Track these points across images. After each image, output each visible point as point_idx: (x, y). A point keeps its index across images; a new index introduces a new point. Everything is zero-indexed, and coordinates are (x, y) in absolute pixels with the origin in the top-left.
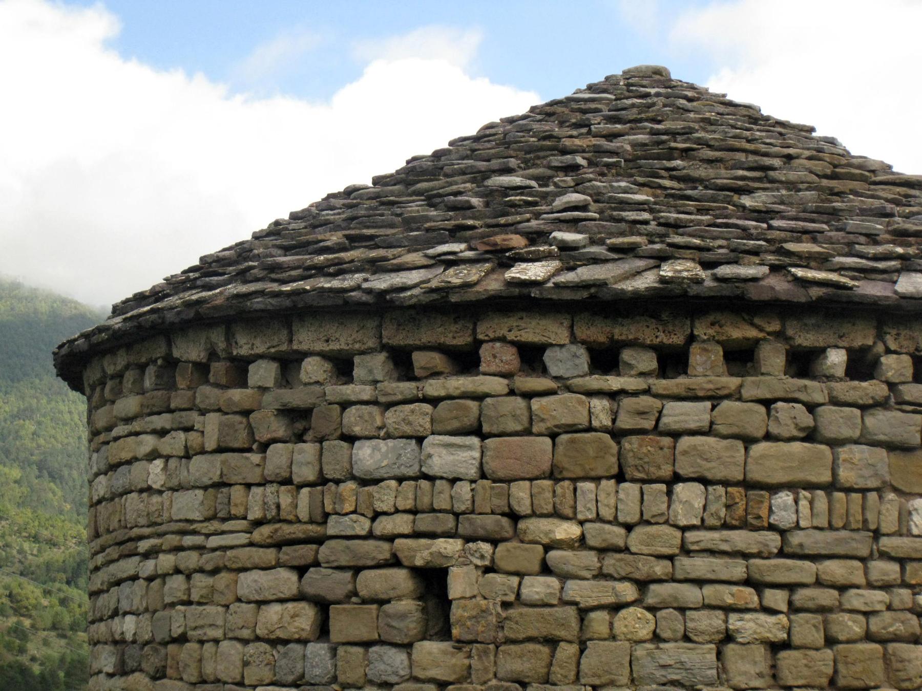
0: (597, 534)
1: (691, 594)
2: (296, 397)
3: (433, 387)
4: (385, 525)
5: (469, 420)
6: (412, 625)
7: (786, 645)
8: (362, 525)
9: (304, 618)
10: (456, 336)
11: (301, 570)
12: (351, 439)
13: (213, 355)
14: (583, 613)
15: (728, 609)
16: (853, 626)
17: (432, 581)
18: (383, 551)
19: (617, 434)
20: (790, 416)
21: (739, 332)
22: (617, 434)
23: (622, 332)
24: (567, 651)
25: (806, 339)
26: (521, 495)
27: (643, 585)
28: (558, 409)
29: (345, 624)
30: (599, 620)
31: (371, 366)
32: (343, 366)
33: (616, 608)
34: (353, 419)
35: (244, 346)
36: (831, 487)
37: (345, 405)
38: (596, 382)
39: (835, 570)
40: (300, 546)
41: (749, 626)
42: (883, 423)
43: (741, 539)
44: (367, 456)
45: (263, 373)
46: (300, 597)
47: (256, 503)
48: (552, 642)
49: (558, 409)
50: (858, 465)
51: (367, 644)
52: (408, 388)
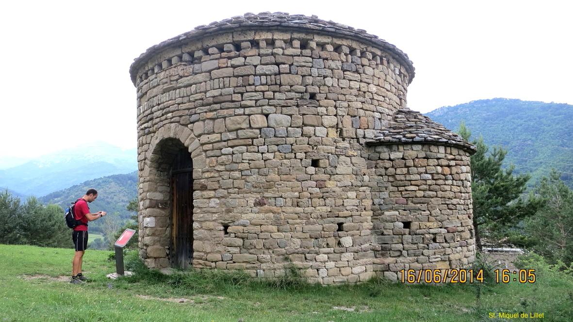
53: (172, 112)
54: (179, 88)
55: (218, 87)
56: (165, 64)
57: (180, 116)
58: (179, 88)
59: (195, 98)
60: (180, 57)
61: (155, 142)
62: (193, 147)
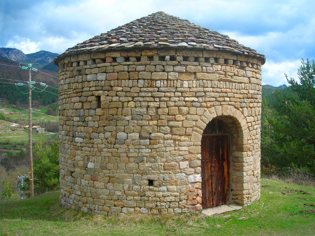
1: (141, 99)
3: (99, 65)
4: (92, 89)
5: (104, 70)
6: (95, 106)
7: (159, 108)
10: (102, 56)
12: (87, 75)
13: (69, 62)
14: (123, 103)
15: (148, 102)
16: (172, 104)
17: (99, 98)
19: (129, 72)
20: (159, 68)
21: (150, 54)
22: (129, 72)
23: (129, 54)
24: (120, 109)
25: (162, 54)
26: (112, 83)
27: (133, 98)
28: (118, 68)
30: (125, 104)
31: (89, 62)
33: (129, 102)
35: (73, 60)
36: (167, 80)
37: (86, 69)
38: (125, 63)
39: (168, 94)
40: (79, 93)
41: (152, 104)
42: (178, 68)
43: (150, 89)
44: (89, 77)
45: (75, 64)
47: (74, 86)
48: (118, 108)
49: (118, 68)
50: (172, 75)
51: (89, 109)
52: (94, 66)
53: (229, 97)
54: (235, 82)
55: (253, 89)
56: (222, 61)
57: (235, 102)
58: (235, 82)
59: (244, 92)
60: (234, 61)
61: (211, 115)
62: (243, 123)
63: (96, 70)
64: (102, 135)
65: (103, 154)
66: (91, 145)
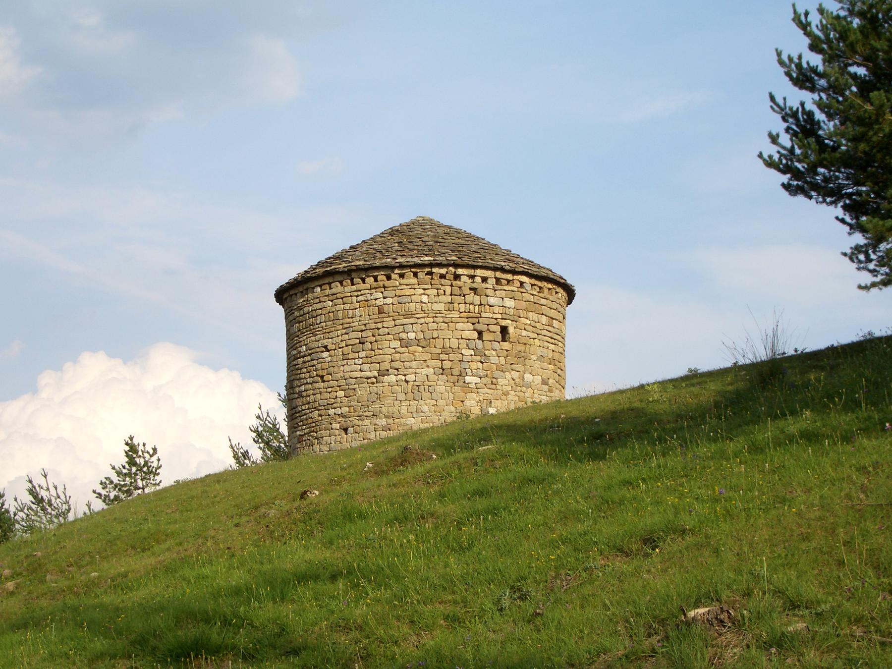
0: (533, 324)
2: (474, 285)
8: (491, 316)
9: (476, 335)
11: (473, 324)
17: (504, 330)
18: (495, 322)
26: (521, 313)
29: (486, 336)
32: (484, 280)
34: (489, 292)
40: (474, 319)
43: (550, 328)
44: (492, 300)
46: (474, 330)
63: (503, 293)
64: (508, 375)
65: (510, 397)
66: (493, 387)
